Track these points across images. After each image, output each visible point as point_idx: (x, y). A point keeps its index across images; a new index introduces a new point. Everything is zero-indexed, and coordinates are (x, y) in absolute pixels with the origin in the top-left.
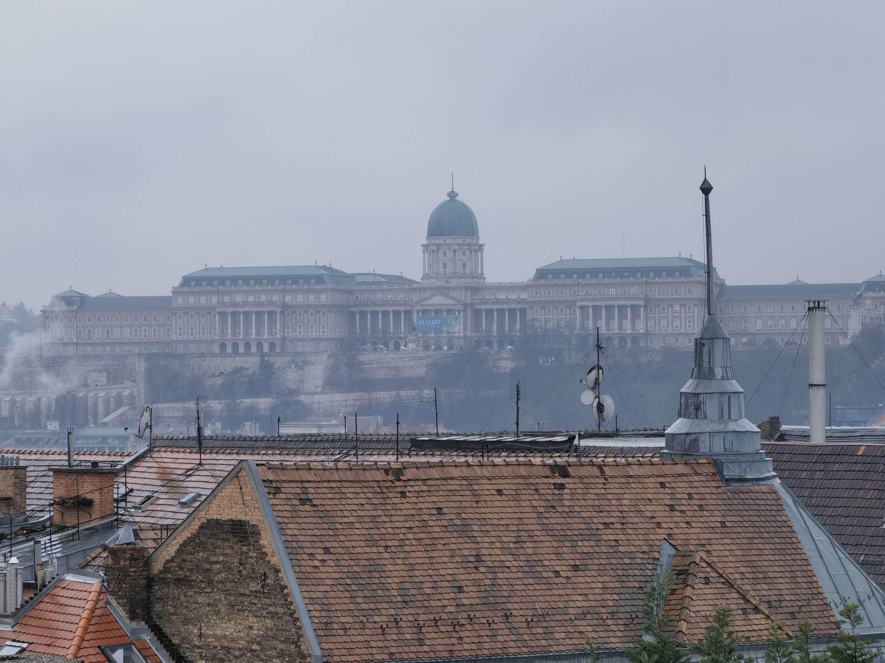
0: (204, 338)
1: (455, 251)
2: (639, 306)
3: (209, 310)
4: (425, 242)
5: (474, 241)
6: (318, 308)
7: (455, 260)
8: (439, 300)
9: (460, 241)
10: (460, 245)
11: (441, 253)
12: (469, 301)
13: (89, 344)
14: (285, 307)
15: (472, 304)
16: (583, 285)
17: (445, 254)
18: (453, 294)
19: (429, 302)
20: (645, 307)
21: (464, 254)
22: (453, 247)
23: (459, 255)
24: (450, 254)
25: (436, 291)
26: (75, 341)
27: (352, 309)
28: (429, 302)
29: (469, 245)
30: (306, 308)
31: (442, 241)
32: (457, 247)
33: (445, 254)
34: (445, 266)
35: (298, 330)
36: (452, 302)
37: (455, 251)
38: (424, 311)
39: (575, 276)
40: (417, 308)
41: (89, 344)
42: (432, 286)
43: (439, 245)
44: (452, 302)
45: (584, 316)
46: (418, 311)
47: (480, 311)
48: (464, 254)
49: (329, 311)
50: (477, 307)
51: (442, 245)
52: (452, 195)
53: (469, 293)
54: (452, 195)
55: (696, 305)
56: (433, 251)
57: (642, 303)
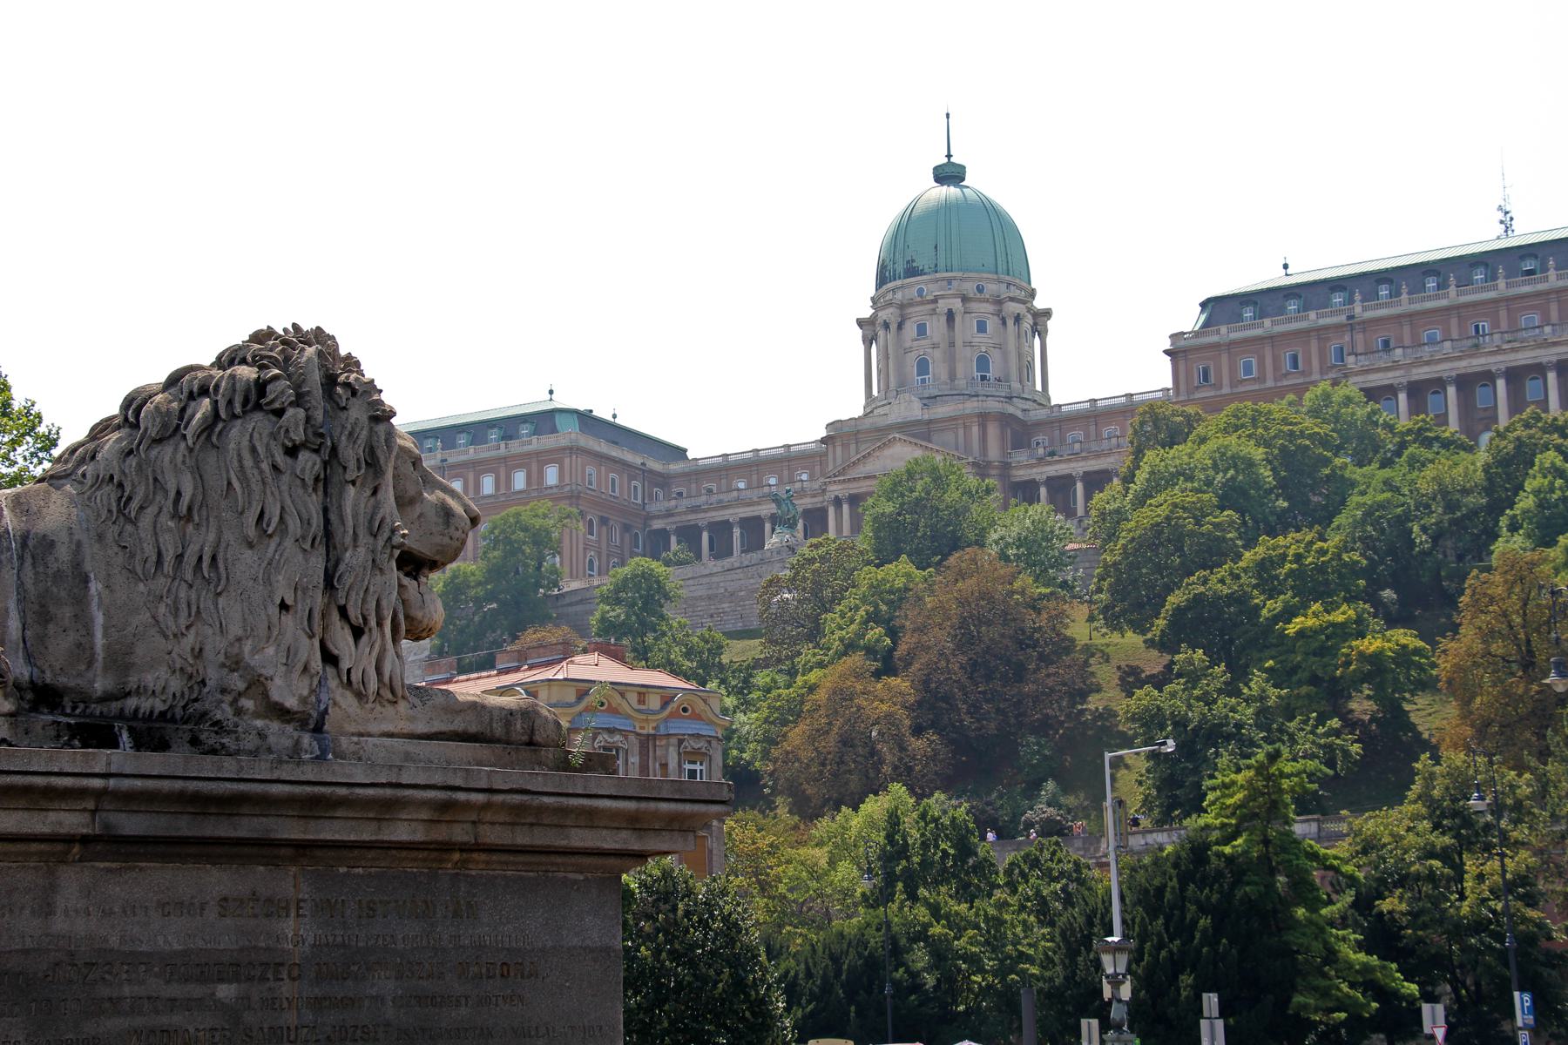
1: (950, 316)
4: (867, 312)
5: (1014, 292)
7: (952, 344)
9: (969, 288)
11: (910, 329)
16: (1367, 325)
17: (922, 330)
21: (982, 327)
22: (943, 306)
23: (966, 328)
27: (657, 525)
32: (957, 304)
33: (922, 330)
37: (950, 316)
38: (855, 500)
39: (1337, 299)
43: (902, 307)
48: (982, 327)
50: (1021, 475)
51: (911, 304)
52: (949, 174)
53: (993, 431)
54: (949, 174)
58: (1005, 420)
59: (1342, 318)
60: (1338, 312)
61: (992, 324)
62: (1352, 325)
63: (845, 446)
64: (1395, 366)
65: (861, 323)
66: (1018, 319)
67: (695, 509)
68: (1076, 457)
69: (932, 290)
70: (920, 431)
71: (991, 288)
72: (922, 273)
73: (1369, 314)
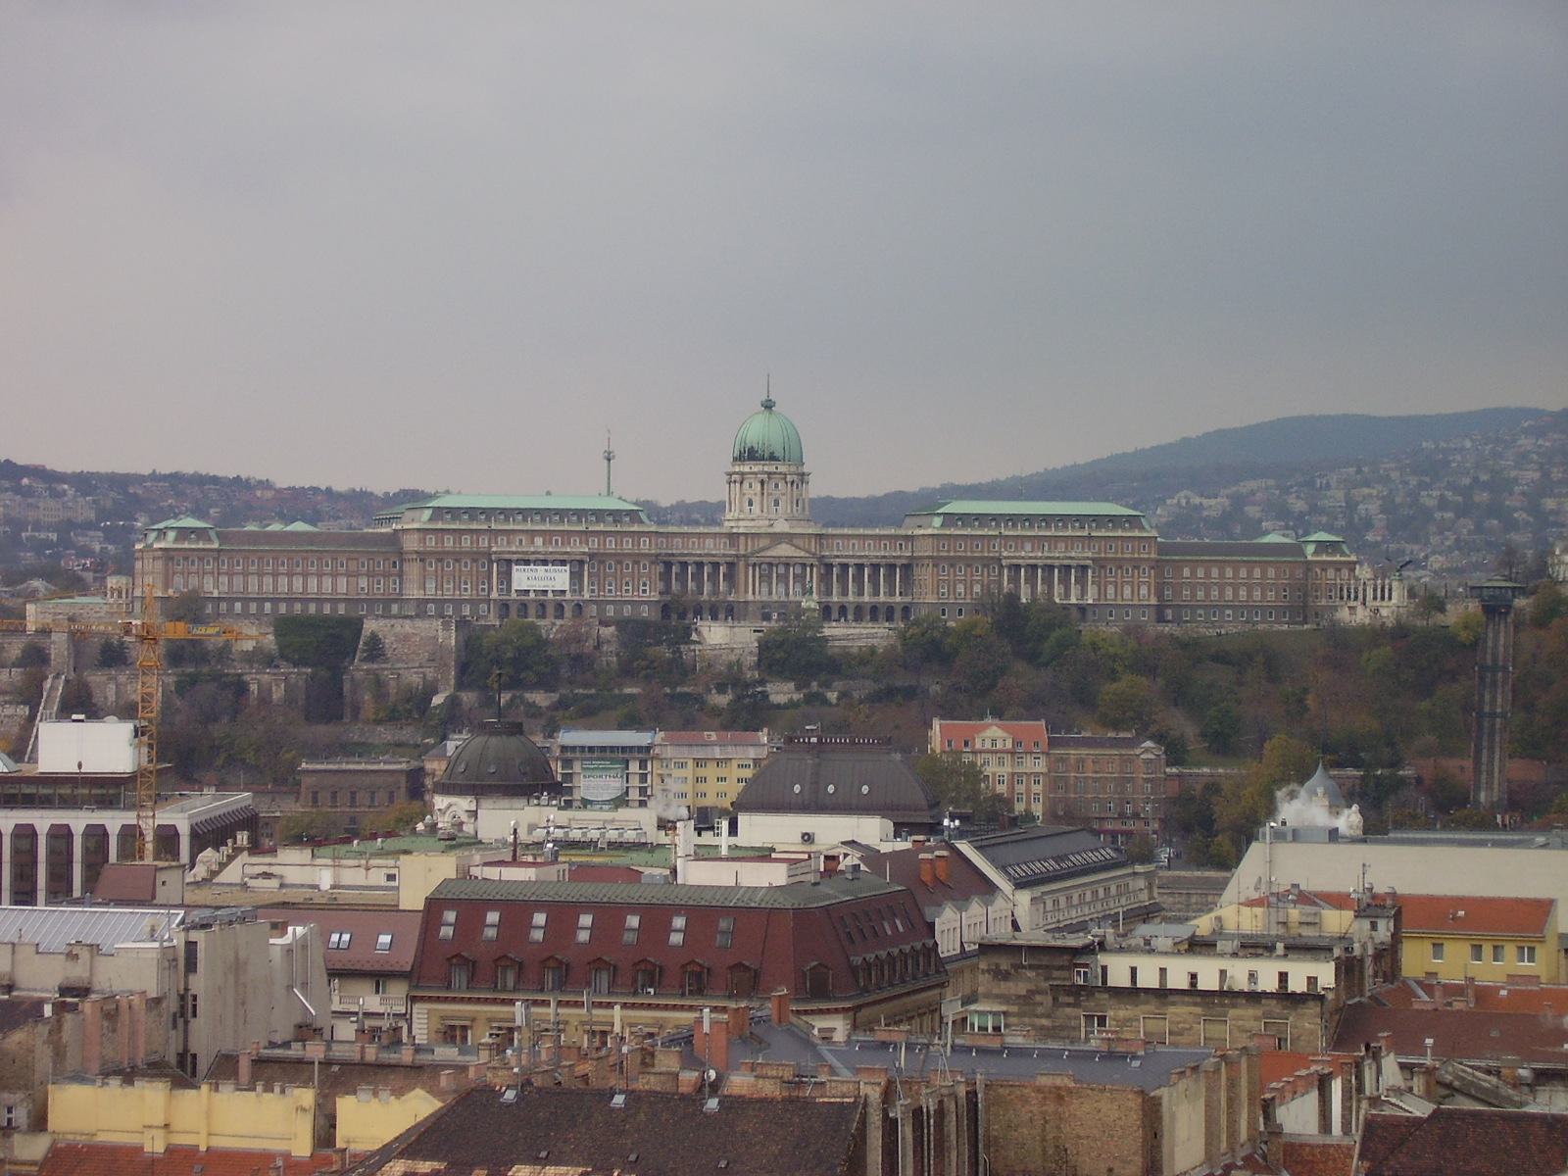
0: (466, 595)
2: (1084, 568)
3: (475, 556)
6: (636, 558)
8: (784, 550)
13: (238, 599)
14: (592, 556)
15: (823, 556)
18: (795, 541)
19: (769, 553)
25: (778, 538)
26: (216, 595)
28: (769, 553)
30: (620, 558)
31: (773, 469)
32: (795, 477)
33: (777, 486)
34: (777, 503)
35: (607, 587)
36: (802, 554)
37: (792, 483)
40: (752, 560)
41: (238, 599)
42: (771, 530)
43: (769, 474)
44: (802, 554)
45: (1014, 580)
46: (754, 565)
47: (831, 566)
49: (652, 563)
50: (827, 561)
51: (775, 473)
52: (768, 406)
55: (1153, 568)
56: (762, 482)
57: (1089, 562)
59: (997, 533)
60: (994, 530)
63: (753, 540)
67: (673, 555)
68: (853, 557)
69: (782, 469)
70: (788, 538)
72: (777, 459)
73: (1007, 533)
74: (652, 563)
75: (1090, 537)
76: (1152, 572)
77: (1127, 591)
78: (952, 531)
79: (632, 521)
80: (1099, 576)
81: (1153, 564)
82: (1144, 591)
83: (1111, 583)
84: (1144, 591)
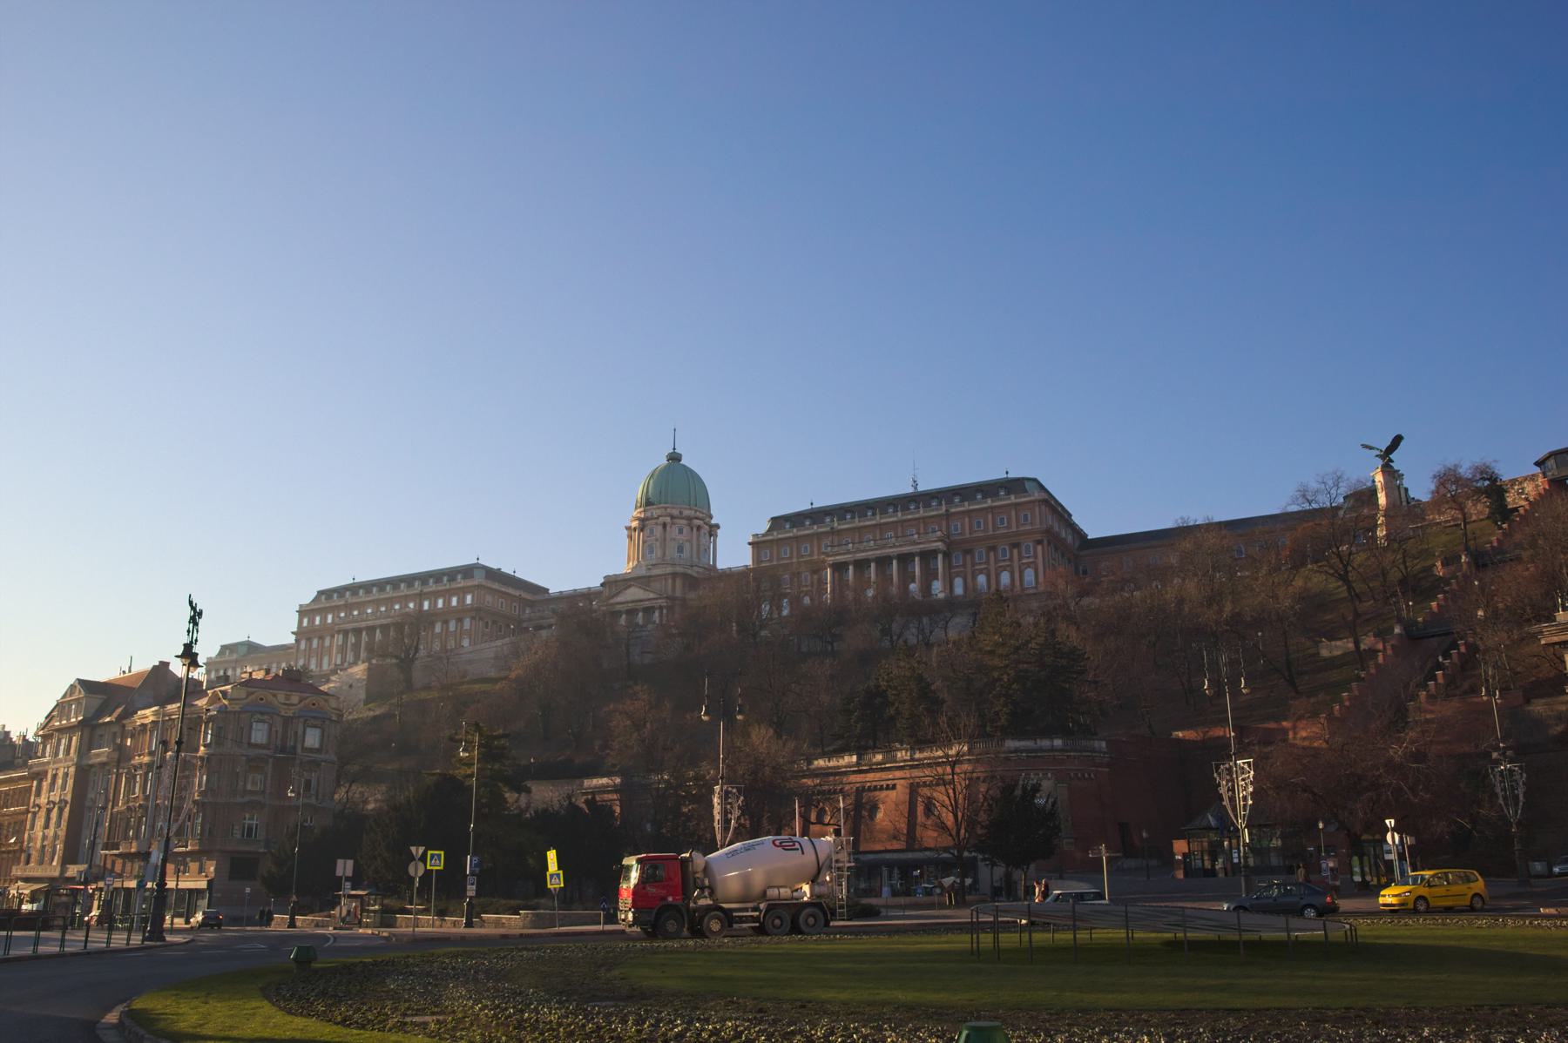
1: (664, 525)
2: (934, 553)
8: (634, 593)
9: (675, 512)
10: (672, 517)
11: (647, 531)
12: (678, 594)
16: (839, 532)
20: (947, 555)
21: (681, 531)
23: (673, 532)
24: (658, 530)
29: (689, 519)
32: (668, 519)
34: (651, 552)
36: (652, 596)
52: (674, 458)
53: (679, 582)
54: (674, 458)
55: (1039, 542)
57: (939, 545)
58: (685, 576)
61: (686, 530)
62: (833, 532)
64: (848, 552)
65: (628, 528)
66: (699, 528)
69: (656, 513)
71: (687, 513)
74: (473, 618)
75: (948, 516)
76: (1039, 548)
77: (1005, 578)
78: (776, 535)
79: (465, 577)
80: (964, 565)
81: (1038, 537)
82: (1029, 575)
83: (981, 572)
84: (1029, 575)
